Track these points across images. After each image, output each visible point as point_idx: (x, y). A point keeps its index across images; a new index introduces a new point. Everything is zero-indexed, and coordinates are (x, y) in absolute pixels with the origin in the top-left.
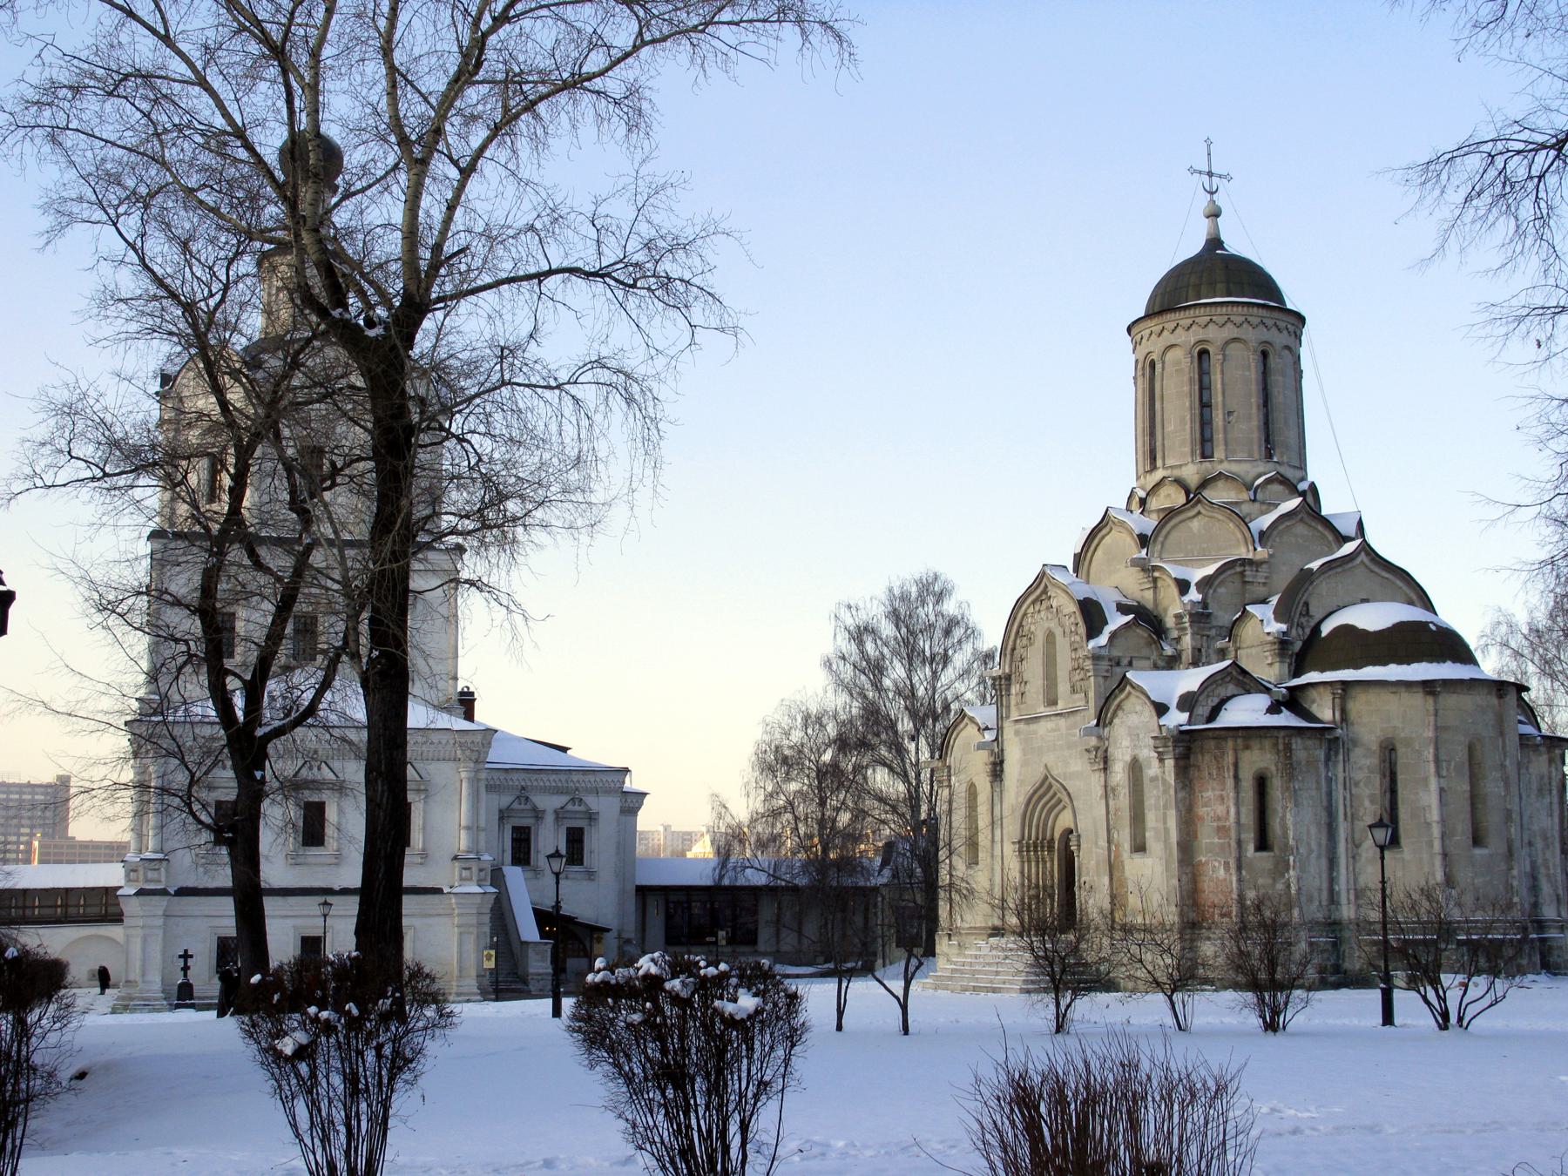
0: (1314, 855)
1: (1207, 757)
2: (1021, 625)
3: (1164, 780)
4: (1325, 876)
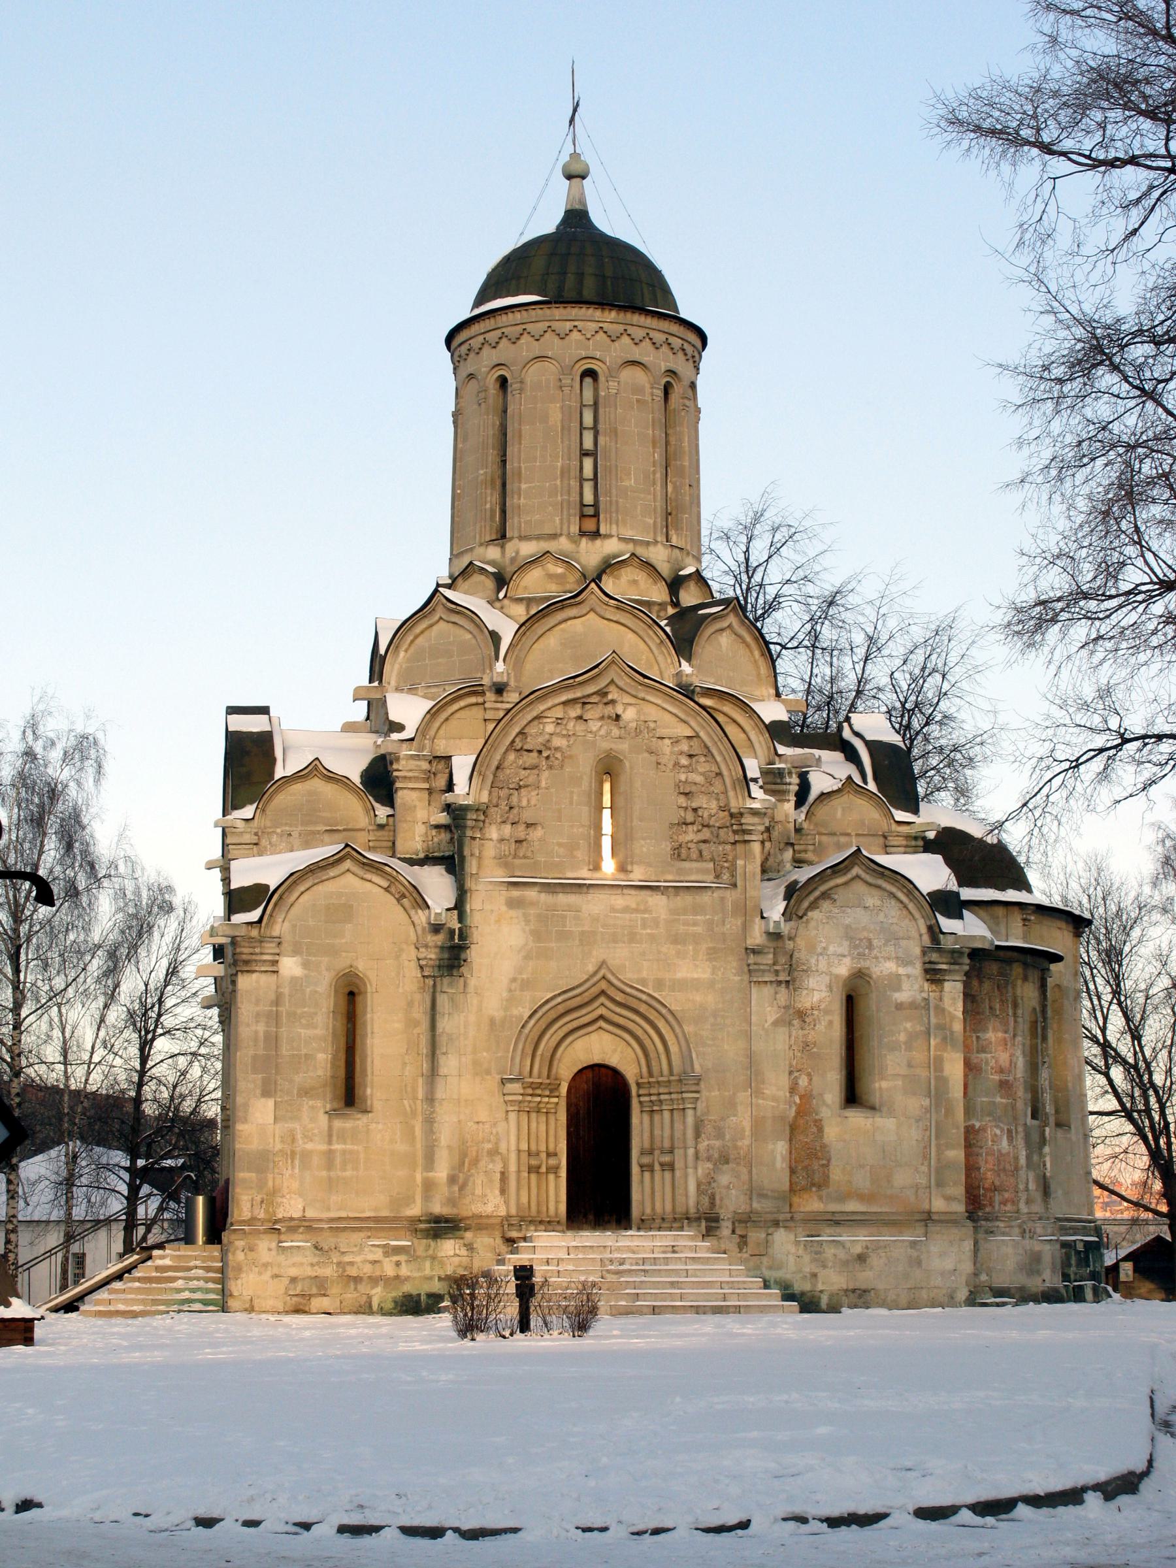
1: (987, 985)
3: (940, 1010)
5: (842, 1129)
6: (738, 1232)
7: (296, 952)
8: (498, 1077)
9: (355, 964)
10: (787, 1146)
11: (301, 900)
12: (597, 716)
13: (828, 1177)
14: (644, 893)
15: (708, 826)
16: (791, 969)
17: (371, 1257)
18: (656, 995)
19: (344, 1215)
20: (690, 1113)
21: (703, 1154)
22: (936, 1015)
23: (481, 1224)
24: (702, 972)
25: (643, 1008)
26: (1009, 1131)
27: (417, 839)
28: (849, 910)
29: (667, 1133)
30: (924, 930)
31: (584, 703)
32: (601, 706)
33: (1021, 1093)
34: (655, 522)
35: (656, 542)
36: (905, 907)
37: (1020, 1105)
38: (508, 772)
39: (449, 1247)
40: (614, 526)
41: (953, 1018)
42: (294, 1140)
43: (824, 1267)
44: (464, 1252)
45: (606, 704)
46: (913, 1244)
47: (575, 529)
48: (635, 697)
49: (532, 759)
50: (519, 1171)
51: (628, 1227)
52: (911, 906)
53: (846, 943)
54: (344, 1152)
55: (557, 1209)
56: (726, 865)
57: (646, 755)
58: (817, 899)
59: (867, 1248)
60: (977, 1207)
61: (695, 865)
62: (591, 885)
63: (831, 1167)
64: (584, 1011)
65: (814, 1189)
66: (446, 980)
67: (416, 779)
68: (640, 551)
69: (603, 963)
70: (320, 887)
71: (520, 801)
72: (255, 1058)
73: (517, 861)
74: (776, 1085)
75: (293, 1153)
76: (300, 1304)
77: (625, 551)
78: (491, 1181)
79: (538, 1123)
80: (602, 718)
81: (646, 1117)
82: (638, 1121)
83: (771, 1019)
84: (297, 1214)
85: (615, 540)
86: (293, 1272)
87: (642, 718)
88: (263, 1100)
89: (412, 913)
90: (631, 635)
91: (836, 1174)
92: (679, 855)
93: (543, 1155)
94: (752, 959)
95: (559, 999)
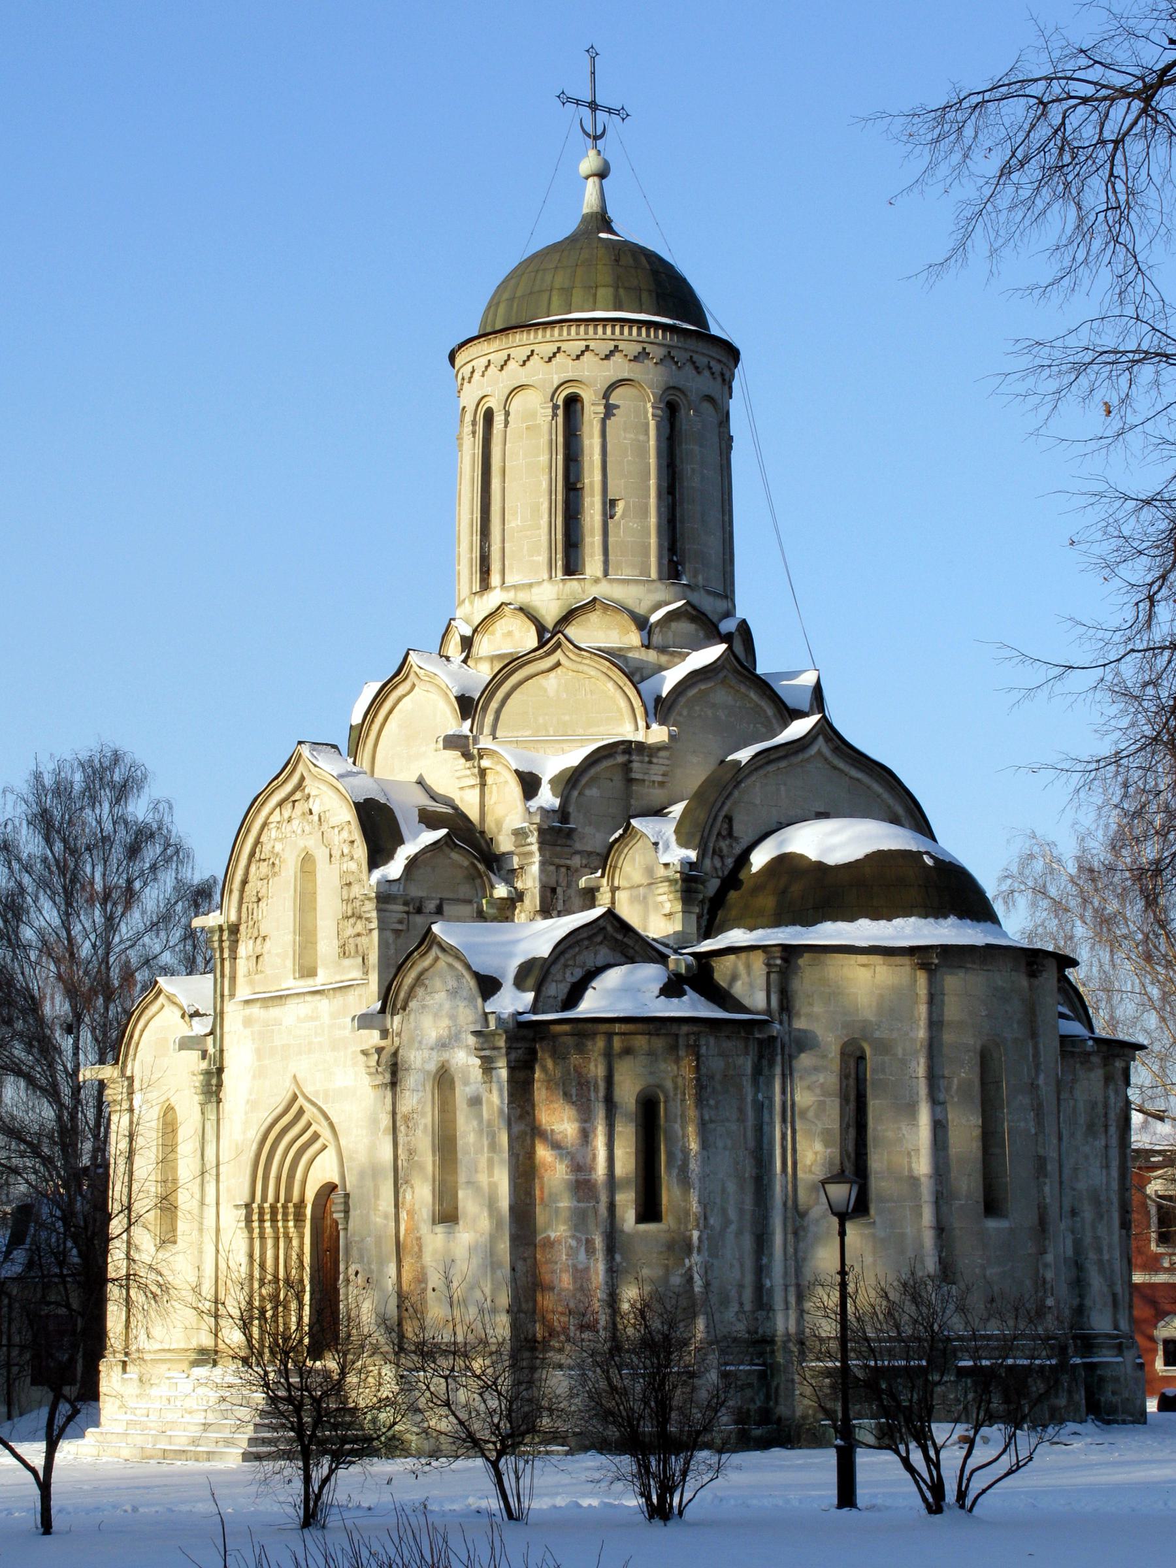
0: (733, 1228)
2: (257, 842)
4: (749, 1263)
18: (324, 1107)
31: (294, 802)
62: (288, 995)
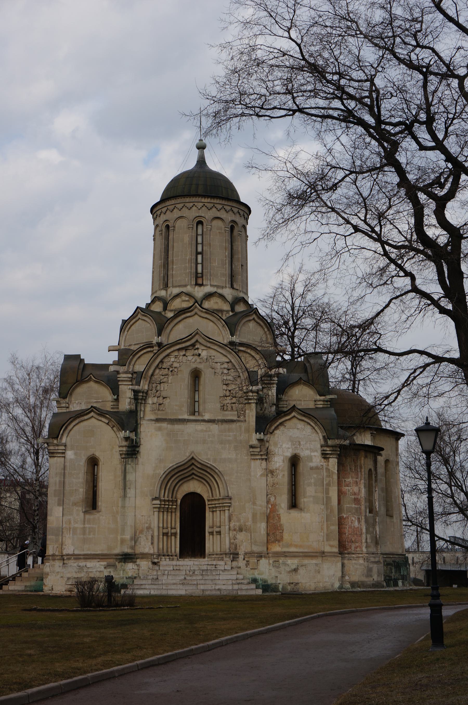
2: (162, 362)
3: (328, 470)
5: (287, 517)
6: (246, 559)
7: (72, 449)
8: (151, 498)
9: (95, 453)
10: (266, 525)
11: (74, 429)
12: (191, 354)
13: (283, 537)
14: (210, 424)
15: (235, 397)
16: (267, 454)
17: (99, 570)
18: (214, 465)
19: (89, 552)
20: (227, 511)
21: (232, 528)
22: (326, 471)
23: (144, 556)
24: (233, 455)
25: (208, 470)
26: (359, 519)
27: (127, 403)
28: (291, 430)
29: (218, 520)
30: (321, 438)
32: (193, 350)
33: (363, 503)
34: (226, 280)
35: (226, 287)
36: (314, 428)
37: (363, 508)
38: (156, 377)
39: (130, 566)
40: (209, 281)
41: (333, 473)
42: (70, 523)
43: (281, 573)
44: (136, 567)
45: (195, 350)
46: (316, 565)
47: (194, 282)
48: (206, 346)
49: (166, 371)
50: (159, 535)
51: (204, 558)
52: (316, 428)
53: (290, 443)
54: (90, 528)
55: (175, 550)
56: (242, 412)
57: (210, 369)
58: (278, 426)
59: (298, 566)
60: (343, 549)
61: (230, 412)
63: (284, 533)
64: (185, 471)
65: (277, 542)
66: (130, 460)
67: (126, 381)
68: (220, 291)
69: (193, 452)
70: (82, 424)
71: (160, 388)
72: (55, 491)
73: (160, 412)
74: (261, 501)
75: (70, 528)
76: (71, 588)
77: (213, 290)
78: (147, 539)
79: (167, 516)
80: (193, 355)
81: (211, 513)
82: (208, 515)
83: (259, 474)
84: (71, 552)
85: (209, 286)
86: (69, 575)
87: (209, 355)
88: (58, 507)
89: (117, 433)
90: (211, 323)
91: (286, 536)
92: (223, 409)
93: (170, 529)
94: (251, 450)
95: (175, 467)
